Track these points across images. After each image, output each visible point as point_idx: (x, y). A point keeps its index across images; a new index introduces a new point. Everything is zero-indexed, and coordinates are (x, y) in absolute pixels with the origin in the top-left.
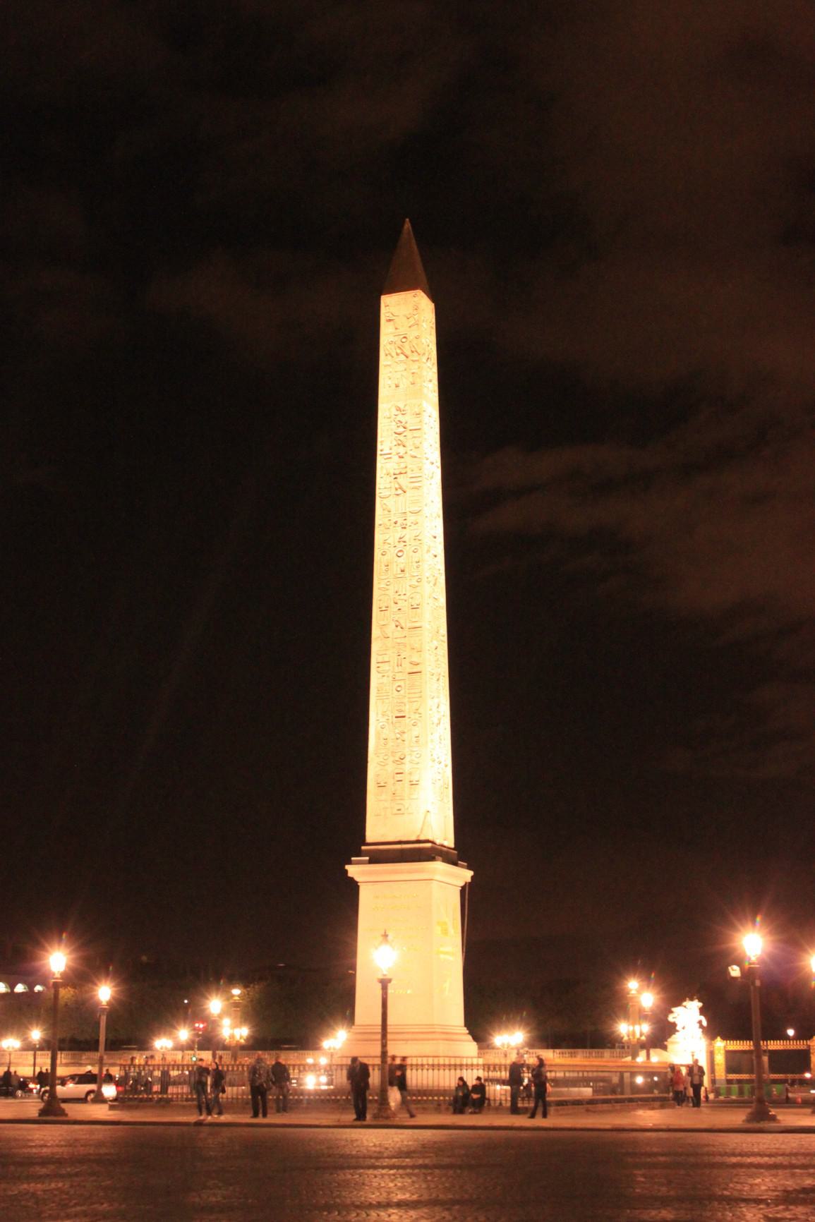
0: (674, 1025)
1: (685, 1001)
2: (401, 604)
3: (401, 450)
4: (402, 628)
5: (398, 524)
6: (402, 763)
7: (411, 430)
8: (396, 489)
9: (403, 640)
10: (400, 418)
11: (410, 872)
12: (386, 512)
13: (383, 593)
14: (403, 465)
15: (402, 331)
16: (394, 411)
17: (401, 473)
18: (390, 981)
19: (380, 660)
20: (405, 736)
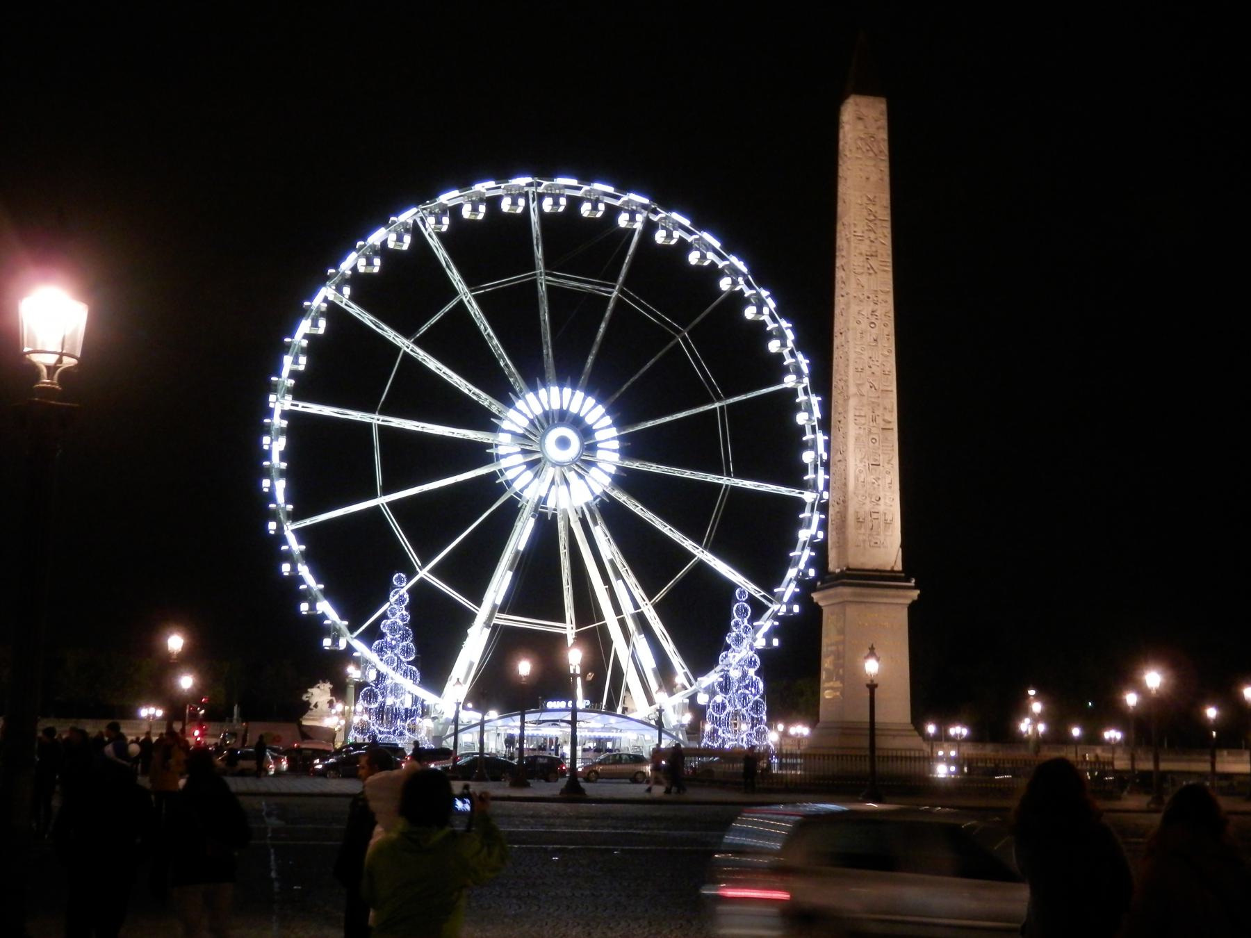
0: (307, 704)
1: (319, 683)
2: (874, 369)
3: (872, 236)
4: (875, 389)
5: (871, 299)
6: (877, 504)
7: (881, 220)
8: (868, 269)
9: (876, 400)
10: (871, 207)
11: (893, 597)
12: (860, 287)
13: (859, 356)
14: (874, 249)
15: (872, 130)
16: (865, 200)
17: (872, 256)
18: (876, 686)
19: (857, 414)
20: (880, 482)
